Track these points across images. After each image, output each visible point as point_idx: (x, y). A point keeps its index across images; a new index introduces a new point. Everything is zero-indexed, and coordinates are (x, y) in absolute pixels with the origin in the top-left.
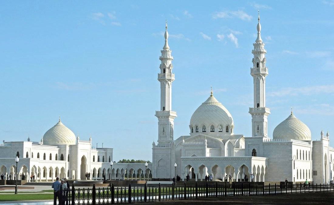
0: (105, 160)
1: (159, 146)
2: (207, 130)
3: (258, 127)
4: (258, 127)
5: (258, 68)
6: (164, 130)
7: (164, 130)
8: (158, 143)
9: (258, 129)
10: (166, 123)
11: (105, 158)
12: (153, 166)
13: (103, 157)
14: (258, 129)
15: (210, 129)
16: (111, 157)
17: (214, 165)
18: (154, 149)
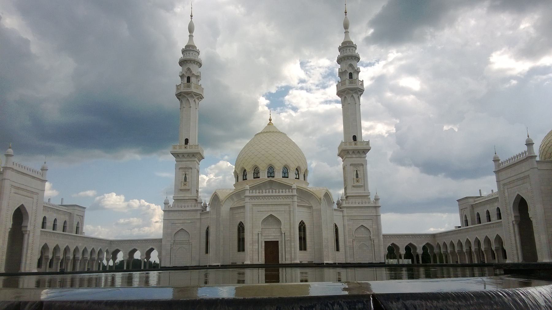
0: (68, 228)
1: (176, 205)
2: (276, 174)
3: (357, 173)
4: (357, 173)
5: (351, 80)
6: (185, 178)
7: (185, 178)
8: (173, 201)
9: (357, 176)
10: (191, 166)
11: (68, 225)
12: (163, 243)
13: (65, 222)
14: (357, 176)
15: (281, 173)
16: (80, 224)
17: (151, 247)
18: (169, 211)
